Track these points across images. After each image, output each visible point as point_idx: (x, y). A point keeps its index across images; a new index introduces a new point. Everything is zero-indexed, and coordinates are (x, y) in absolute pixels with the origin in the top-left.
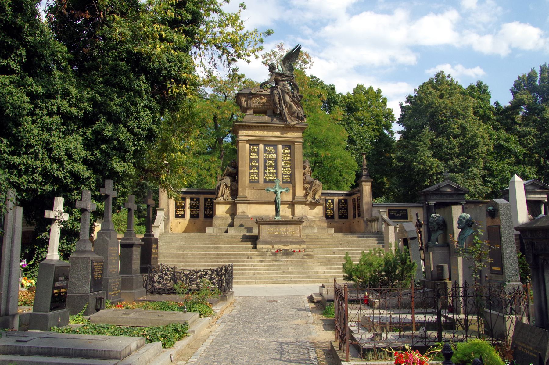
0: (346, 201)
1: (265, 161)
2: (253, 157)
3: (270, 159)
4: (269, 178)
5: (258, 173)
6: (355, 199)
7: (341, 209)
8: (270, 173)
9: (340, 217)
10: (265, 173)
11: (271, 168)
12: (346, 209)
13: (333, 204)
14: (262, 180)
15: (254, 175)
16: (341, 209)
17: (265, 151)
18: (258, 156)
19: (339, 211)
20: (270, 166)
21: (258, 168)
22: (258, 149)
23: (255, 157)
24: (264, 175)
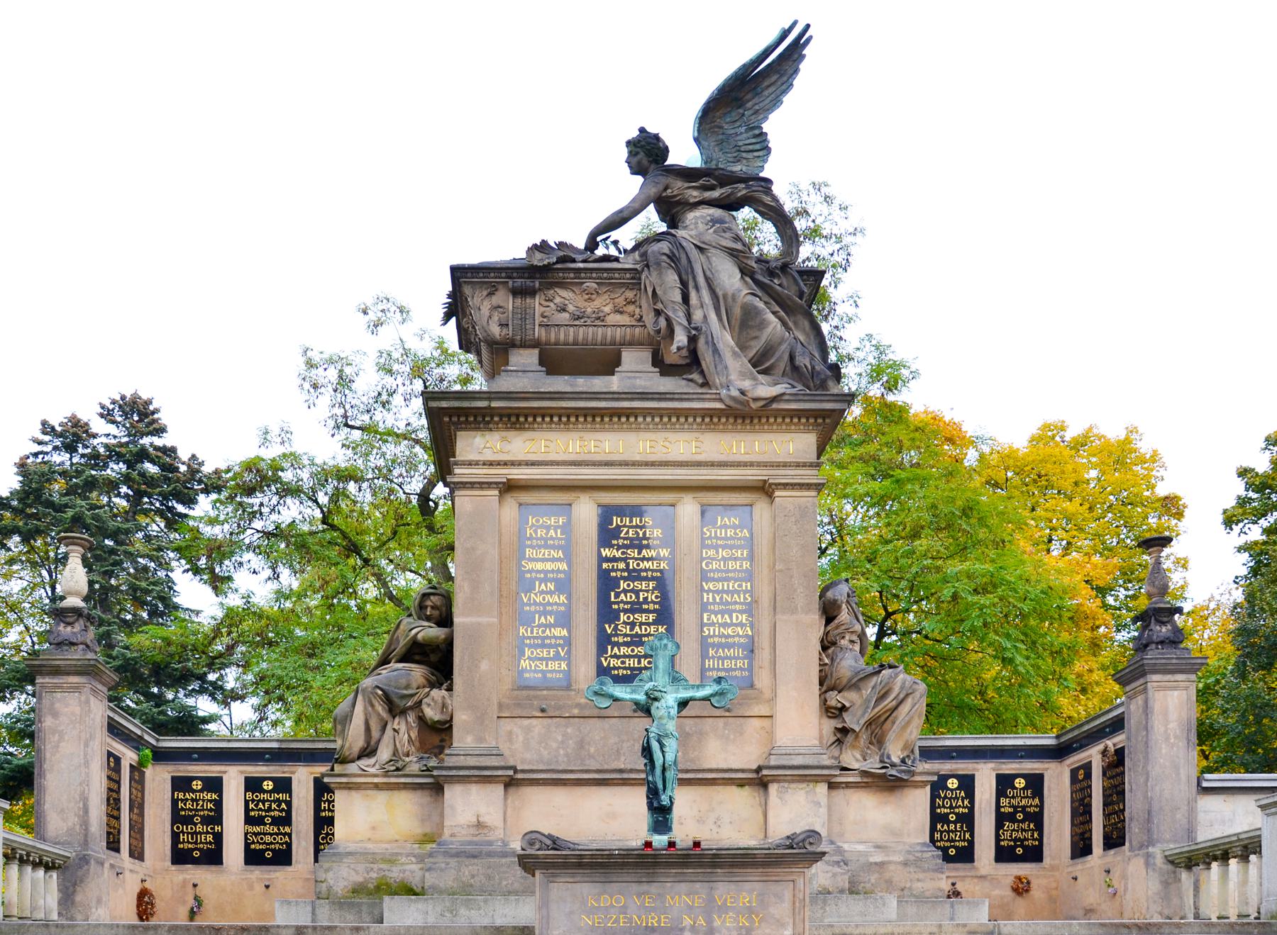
1: (606, 582)
2: (540, 566)
3: (634, 575)
5: (568, 642)
7: (1011, 817)
9: (1004, 855)
10: (604, 642)
13: (970, 795)
14: (585, 671)
16: (1011, 817)
18: (568, 558)
19: (999, 825)
20: (636, 608)
21: (565, 620)
22: (567, 528)
23: (549, 566)
24: (601, 650)
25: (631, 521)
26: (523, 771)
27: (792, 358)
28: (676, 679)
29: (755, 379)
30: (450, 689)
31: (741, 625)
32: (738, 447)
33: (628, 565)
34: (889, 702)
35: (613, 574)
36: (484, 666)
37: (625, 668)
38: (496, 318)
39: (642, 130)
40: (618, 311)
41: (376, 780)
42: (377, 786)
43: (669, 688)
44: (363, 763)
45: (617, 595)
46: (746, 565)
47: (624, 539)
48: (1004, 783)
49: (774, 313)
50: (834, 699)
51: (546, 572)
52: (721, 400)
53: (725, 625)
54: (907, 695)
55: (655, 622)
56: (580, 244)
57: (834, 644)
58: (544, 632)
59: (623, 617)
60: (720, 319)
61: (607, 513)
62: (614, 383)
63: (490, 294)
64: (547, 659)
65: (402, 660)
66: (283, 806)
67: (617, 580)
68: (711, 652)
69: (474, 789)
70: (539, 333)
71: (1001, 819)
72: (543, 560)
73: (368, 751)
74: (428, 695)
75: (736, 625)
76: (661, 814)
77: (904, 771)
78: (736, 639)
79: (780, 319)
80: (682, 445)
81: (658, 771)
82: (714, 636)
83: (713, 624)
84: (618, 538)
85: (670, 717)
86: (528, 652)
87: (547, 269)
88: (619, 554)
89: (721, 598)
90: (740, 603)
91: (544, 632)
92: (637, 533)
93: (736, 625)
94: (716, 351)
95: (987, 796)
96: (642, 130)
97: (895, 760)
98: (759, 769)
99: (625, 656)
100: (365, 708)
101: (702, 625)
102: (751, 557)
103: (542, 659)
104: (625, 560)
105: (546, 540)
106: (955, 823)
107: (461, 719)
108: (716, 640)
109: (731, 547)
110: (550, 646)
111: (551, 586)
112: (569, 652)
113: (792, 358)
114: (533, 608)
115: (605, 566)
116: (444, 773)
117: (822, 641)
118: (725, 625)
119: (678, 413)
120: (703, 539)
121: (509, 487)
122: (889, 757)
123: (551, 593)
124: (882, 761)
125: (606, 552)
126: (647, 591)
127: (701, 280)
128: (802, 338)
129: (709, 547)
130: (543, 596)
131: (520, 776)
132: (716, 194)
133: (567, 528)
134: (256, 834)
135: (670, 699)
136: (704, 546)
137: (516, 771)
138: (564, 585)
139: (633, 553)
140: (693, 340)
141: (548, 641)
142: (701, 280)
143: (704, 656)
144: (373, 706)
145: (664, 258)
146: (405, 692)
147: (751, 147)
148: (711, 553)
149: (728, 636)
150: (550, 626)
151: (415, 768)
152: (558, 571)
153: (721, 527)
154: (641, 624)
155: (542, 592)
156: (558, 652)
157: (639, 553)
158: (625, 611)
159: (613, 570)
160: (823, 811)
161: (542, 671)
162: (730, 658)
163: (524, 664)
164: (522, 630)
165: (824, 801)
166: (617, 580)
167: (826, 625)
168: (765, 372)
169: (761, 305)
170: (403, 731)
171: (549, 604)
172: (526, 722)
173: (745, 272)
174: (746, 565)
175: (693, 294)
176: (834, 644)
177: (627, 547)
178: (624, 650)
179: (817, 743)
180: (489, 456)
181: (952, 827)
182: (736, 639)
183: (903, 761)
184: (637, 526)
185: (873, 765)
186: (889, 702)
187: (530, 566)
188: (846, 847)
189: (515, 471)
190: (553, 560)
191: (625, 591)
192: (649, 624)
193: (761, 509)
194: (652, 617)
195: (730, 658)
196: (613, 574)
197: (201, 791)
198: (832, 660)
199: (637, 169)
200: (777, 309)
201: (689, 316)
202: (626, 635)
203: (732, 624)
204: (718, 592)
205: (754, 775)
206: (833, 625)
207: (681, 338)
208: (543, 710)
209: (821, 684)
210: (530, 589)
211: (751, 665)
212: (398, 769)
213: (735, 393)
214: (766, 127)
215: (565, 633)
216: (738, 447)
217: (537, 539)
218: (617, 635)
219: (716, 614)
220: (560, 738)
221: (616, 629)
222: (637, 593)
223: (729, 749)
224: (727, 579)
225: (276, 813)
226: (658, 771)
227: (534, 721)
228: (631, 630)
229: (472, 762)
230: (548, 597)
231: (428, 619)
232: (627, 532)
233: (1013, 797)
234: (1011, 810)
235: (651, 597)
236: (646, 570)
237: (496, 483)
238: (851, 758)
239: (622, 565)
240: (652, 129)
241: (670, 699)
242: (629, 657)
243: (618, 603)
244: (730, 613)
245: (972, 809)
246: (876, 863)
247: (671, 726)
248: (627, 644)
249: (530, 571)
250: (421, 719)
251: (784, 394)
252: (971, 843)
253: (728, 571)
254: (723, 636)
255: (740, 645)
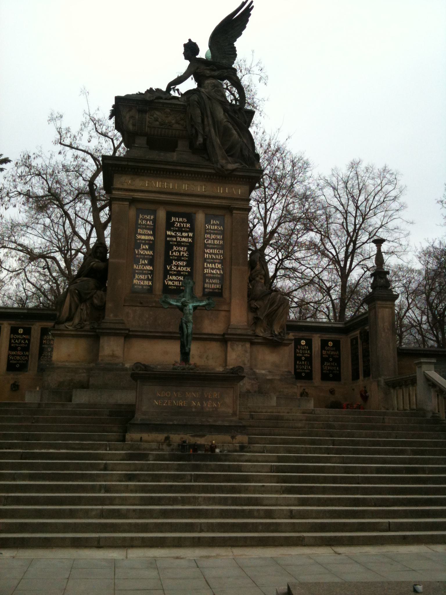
0: (337, 344)
1: (168, 246)
2: (143, 237)
3: (179, 244)
4: (176, 283)
5: (152, 272)
6: (356, 339)
7: (327, 360)
8: (179, 273)
9: (325, 377)
11: (180, 263)
12: (338, 361)
14: (158, 287)
15: (142, 277)
16: (327, 360)
17: (169, 225)
18: (154, 235)
19: (322, 363)
20: (179, 259)
23: (147, 238)
25: (179, 219)
26: (133, 331)
27: (241, 151)
28: (193, 297)
29: (227, 159)
30: (105, 291)
31: (219, 269)
32: (220, 190)
33: (177, 239)
34: (274, 307)
35: (171, 243)
36: (120, 282)
37: (174, 286)
38: (131, 122)
39: (190, 40)
40: (177, 123)
41: (72, 333)
42: (73, 336)
43: (190, 301)
44: (67, 324)
45: (172, 253)
46: (221, 242)
47: (176, 227)
48: (324, 343)
49: (235, 130)
50: (255, 304)
51: (145, 240)
52: (214, 169)
53: (213, 269)
54: (281, 305)
55: (186, 266)
56: (164, 89)
57: (254, 279)
58: (143, 267)
59: (174, 263)
60: (215, 131)
61: (169, 215)
62: (174, 156)
63: (130, 111)
64: (144, 280)
65: (86, 276)
66: (27, 342)
67: (173, 245)
68: (207, 281)
69: (112, 338)
70: (147, 129)
71: (323, 360)
72: (145, 235)
73: (70, 319)
74: (95, 293)
75: (217, 269)
76: (185, 355)
77: (280, 339)
78: (217, 275)
79: (237, 132)
80: (200, 188)
81: (185, 337)
82: (208, 273)
83: (208, 268)
84: (174, 227)
85: (190, 314)
86: (136, 276)
87: (151, 102)
88: (173, 234)
89: (212, 257)
90: (219, 259)
91: (143, 267)
92: (181, 225)
93: (217, 269)
94: (213, 146)
95: (317, 349)
96: (190, 40)
97: (276, 333)
98: (224, 335)
99: (174, 280)
100: (70, 299)
101: (205, 268)
102: (223, 239)
103: (142, 280)
104: (176, 237)
105: (146, 225)
106: (304, 361)
107: (109, 305)
108: (209, 275)
109: (216, 234)
110: (145, 274)
111: (147, 247)
112: (152, 277)
113: (241, 151)
114: (140, 256)
115: (168, 239)
116: (101, 331)
117: (249, 278)
118: (213, 269)
119: (198, 173)
120: (206, 230)
121: (133, 201)
122: (274, 332)
123: (146, 250)
124: (271, 333)
125: (169, 233)
126: (184, 251)
127: (209, 113)
128: (245, 141)
129: (208, 233)
130: (144, 251)
131: (131, 333)
132: (216, 73)
133: (154, 221)
134: (13, 355)
135: (191, 306)
136: (206, 233)
137: (129, 331)
138: (152, 246)
139: (179, 234)
140: (205, 140)
141: (144, 272)
142: (209, 113)
143: (204, 282)
144: (73, 297)
145: (195, 103)
146: (87, 292)
147: (230, 53)
148: (209, 236)
149: (214, 274)
150: (145, 265)
151: (87, 328)
152: (150, 240)
153: (213, 225)
154: (181, 266)
155: (143, 249)
156: (148, 277)
157: (181, 234)
158: (175, 260)
159: (171, 241)
160: (248, 355)
161: (142, 285)
162: (214, 284)
163: (135, 281)
164: (135, 266)
165: (249, 350)
166: (173, 245)
167: (251, 270)
168: (231, 156)
169: (231, 126)
170: (84, 309)
171: (146, 255)
172: (134, 308)
173: (225, 111)
174: (221, 242)
175: (206, 120)
176: (254, 279)
177: (177, 231)
178: (174, 278)
179: (246, 324)
180: (126, 186)
181: (303, 363)
182: (217, 275)
183: (279, 334)
184: (181, 222)
185: (268, 335)
186: (274, 307)
187: (139, 237)
188: (257, 371)
189: (136, 194)
190: (148, 235)
191: (175, 251)
192: (184, 266)
193: (228, 220)
194: (185, 263)
195: (214, 284)
196: (171, 243)
197: (18, 346)
198: (253, 287)
199: (187, 57)
200: (237, 128)
201: (204, 129)
202: (175, 271)
203: (215, 269)
204: (210, 254)
205: (220, 337)
206: (254, 271)
207: (200, 140)
208: (141, 303)
209: (249, 296)
210: (138, 247)
211: (222, 287)
212: (81, 328)
213: (219, 167)
214: (236, 44)
215: (151, 268)
216: (220, 190)
217: (142, 225)
218: (172, 271)
219: (209, 263)
220: (147, 316)
221: (171, 268)
222: (180, 252)
223: (212, 326)
224: (214, 248)
225: (23, 345)
226: (185, 337)
227: (137, 308)
228: (177, 268)
229: (112, 326)
230: (146, 252)
231: (97, 258)
232: (177, 225)
233: (328, 350)
234: (327, 356)
235: (185, 255)
236: (184, 242)
237: (128, 199)
238: (260, 332)
239: (174, 239)
240: (193, 40)
241: (191, 306)
242: (176, 281)
243: (172, 256)
244: (215, 263)
245: (311, 354)
246: (269, 380)
247: (190, 318)
248: (175, 275)
249: (140, 239)
250: (92, 304)
251: (237, 168)
252: (311, 371)
253: (214, 245)
254: (211, 273)
255: (217, 278)
